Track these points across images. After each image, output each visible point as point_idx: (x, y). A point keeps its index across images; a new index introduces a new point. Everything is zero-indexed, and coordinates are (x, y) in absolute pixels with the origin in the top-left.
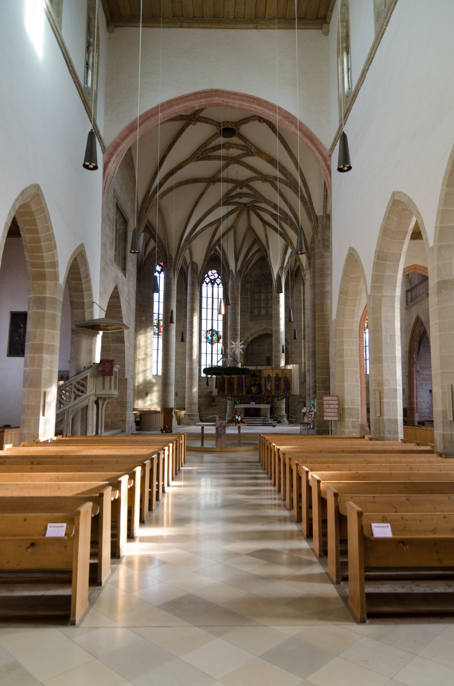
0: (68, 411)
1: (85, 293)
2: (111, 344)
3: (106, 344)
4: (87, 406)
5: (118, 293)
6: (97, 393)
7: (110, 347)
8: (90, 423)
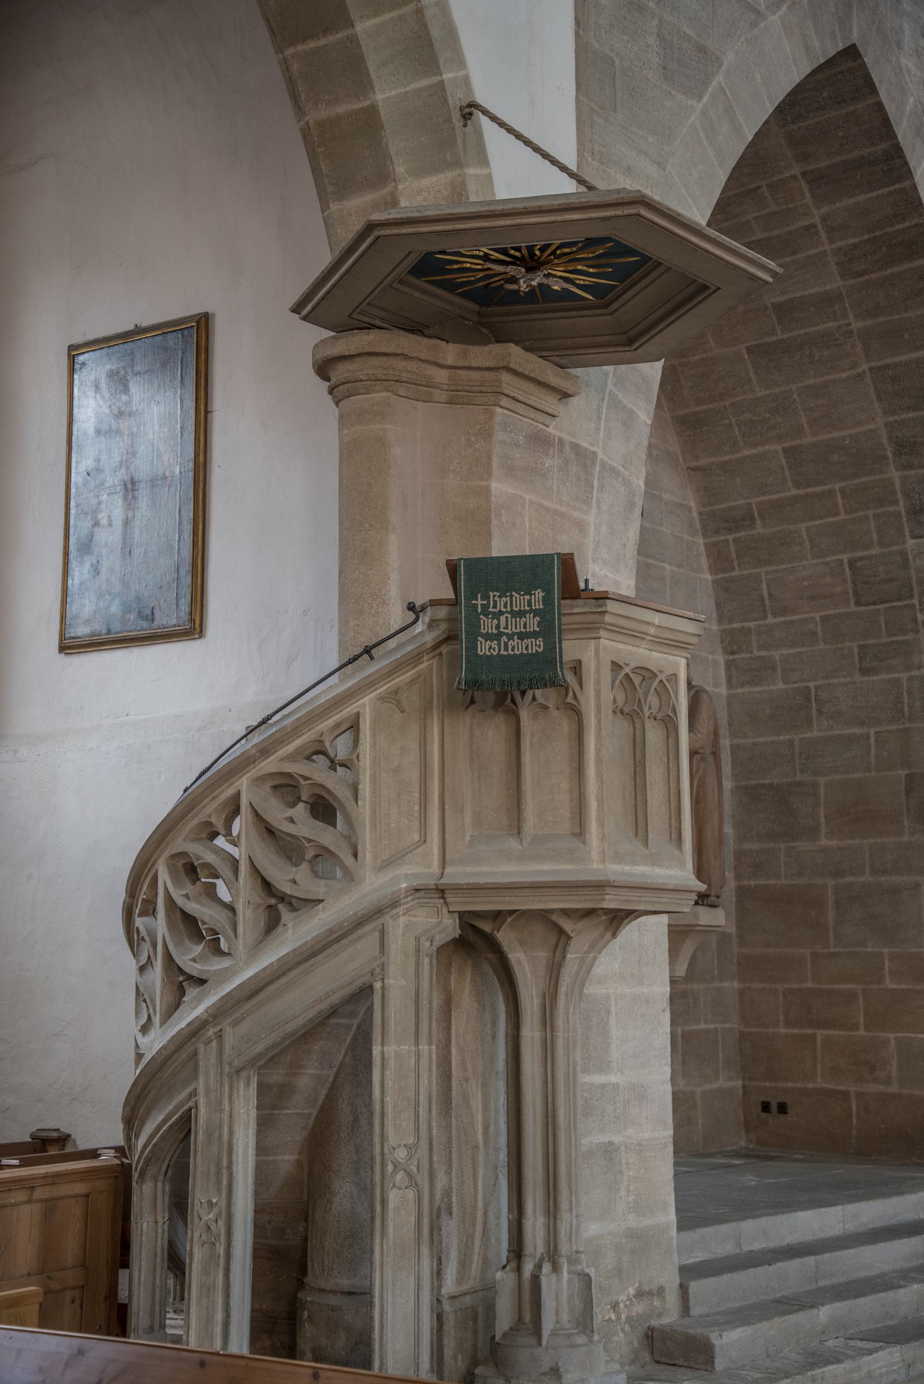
0: (219, 1036)
1: (362, 27)
2: (911, 543)
3: (875, 551)
4: (364, 992)
6: (457, 874)
7: (905, 564)
8: (401, 1154)
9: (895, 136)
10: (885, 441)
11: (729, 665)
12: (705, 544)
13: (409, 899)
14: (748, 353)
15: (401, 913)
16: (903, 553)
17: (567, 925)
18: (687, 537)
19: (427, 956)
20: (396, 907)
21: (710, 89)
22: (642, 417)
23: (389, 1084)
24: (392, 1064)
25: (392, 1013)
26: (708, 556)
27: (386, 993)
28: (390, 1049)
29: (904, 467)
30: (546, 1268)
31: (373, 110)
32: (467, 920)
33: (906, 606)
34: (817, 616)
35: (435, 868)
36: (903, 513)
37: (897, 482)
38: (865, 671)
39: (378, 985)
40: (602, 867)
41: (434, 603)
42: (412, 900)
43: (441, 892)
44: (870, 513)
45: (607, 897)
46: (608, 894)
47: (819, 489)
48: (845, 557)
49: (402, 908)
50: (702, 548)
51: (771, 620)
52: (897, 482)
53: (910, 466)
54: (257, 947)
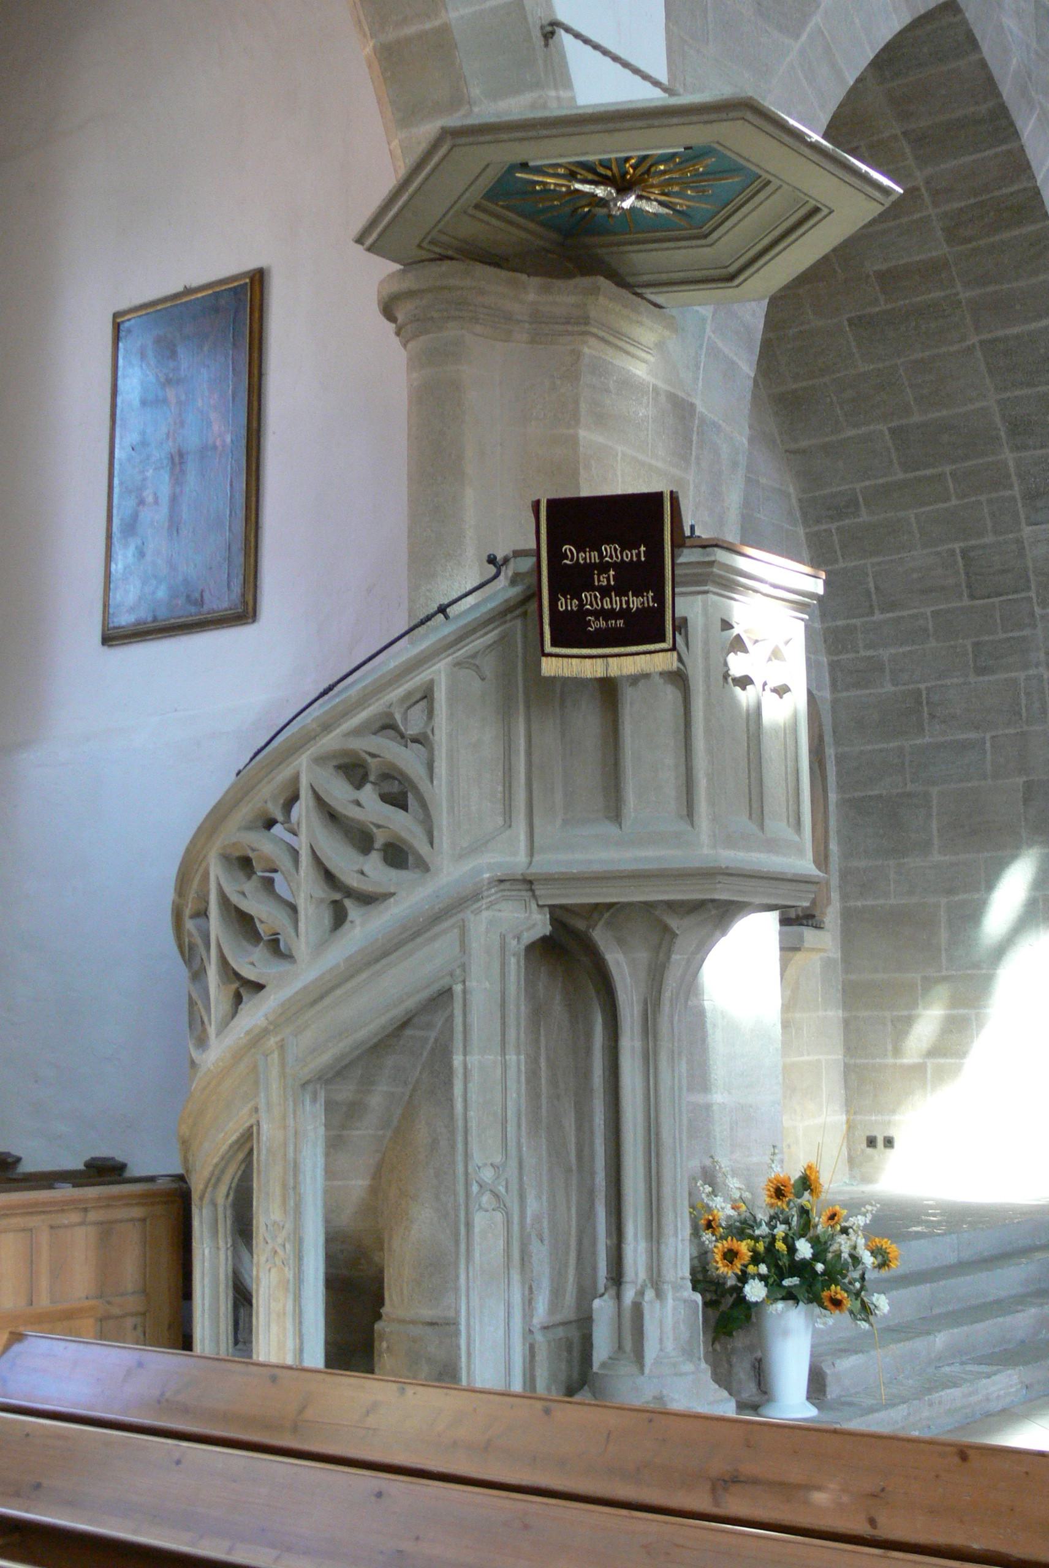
0: (282, 1047)
2: (1027, 531)
3: (989, 539)
5: (990, 86)
7: (1021, 553)
8: (488, 1175)
9: (999, 95)
10: (998, 419)
11: (833, 666)
12: (806, 534)
13: (493, 891)
14: (850, 325)
15: (484, 907)
16: (1019, 542)
17: (673, 923)
18: (786, 526)
19: (514, 955)
20: (479, 900)
21: (808, 29)
22: (744, 368)
23: (473, 1096)
24: (475, 1075)
25: (474, 1019)
26: (809, 546)
27: (467, 997)
28: (474, 1059)
29: (1017, 448)
30: (650, 1294)
31: (444, 30)
32: (559, 916)
33: (1023, 599)
34: (928, 611)
35: (522, 858)
36: (1018, 496)
37: (1011, 464)
38: (981, 671)
39: (458, 988)
40: (712, 852)
41: (517, 554)
42: (496, 892)
43: (528, 883)
44: (983, 498)
45: (718, 886)
46: (719, 882)
47: (929, 472)
48: (957, 546)
49: (484, 901)
50: (803, 538)
51: (878, 616)
52: (1011, 464)
53: (1025, 447)
54: (321, 947)
